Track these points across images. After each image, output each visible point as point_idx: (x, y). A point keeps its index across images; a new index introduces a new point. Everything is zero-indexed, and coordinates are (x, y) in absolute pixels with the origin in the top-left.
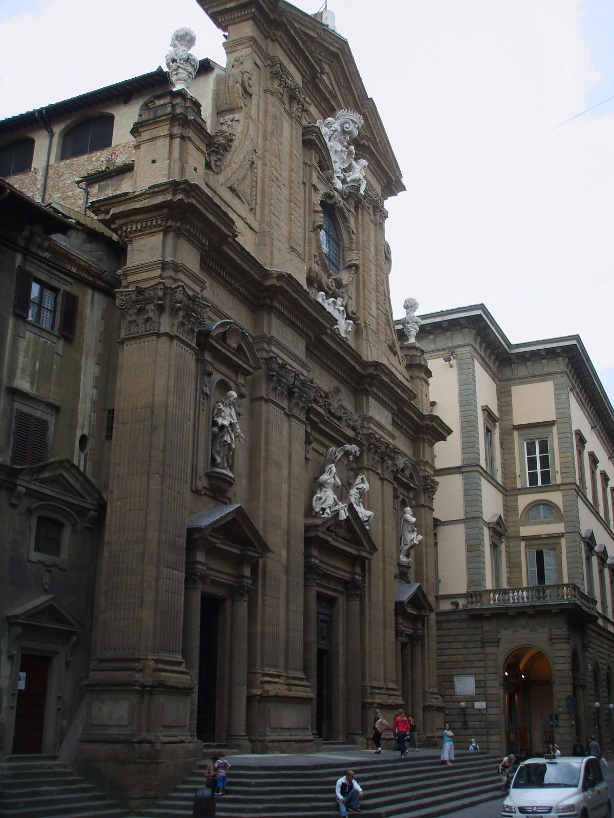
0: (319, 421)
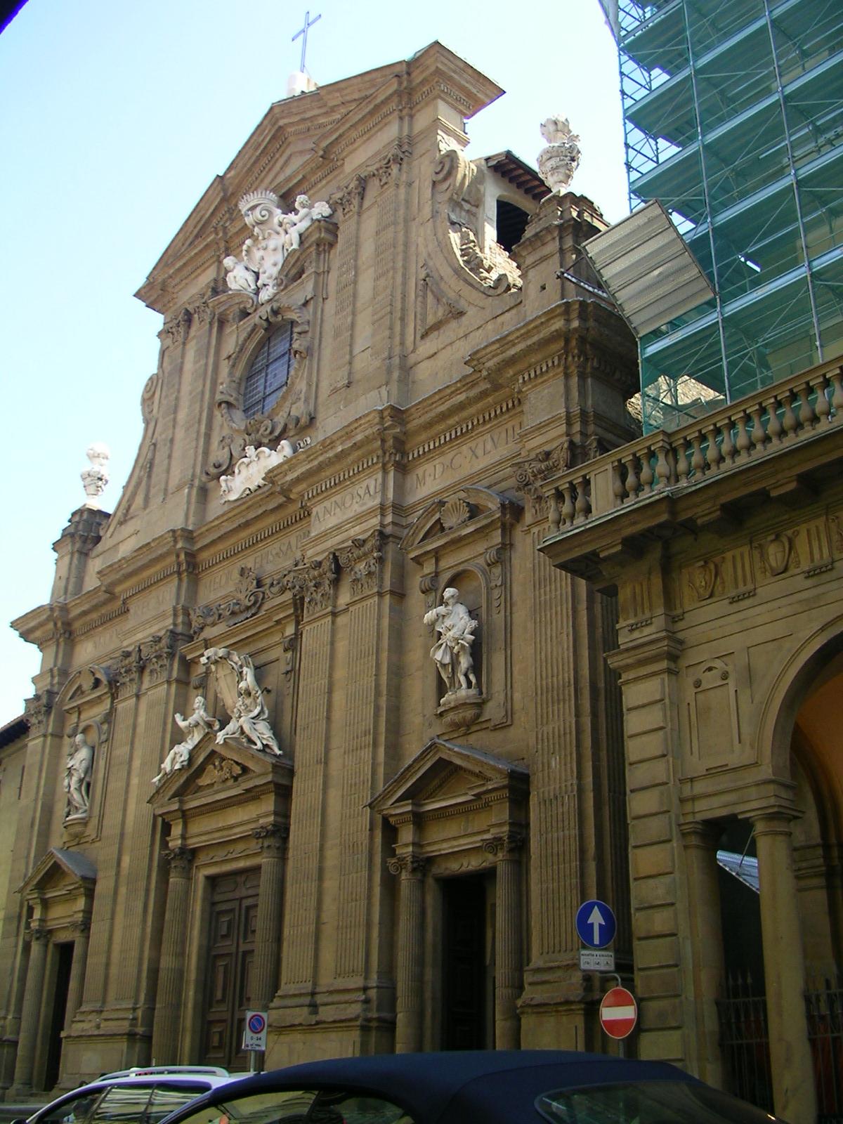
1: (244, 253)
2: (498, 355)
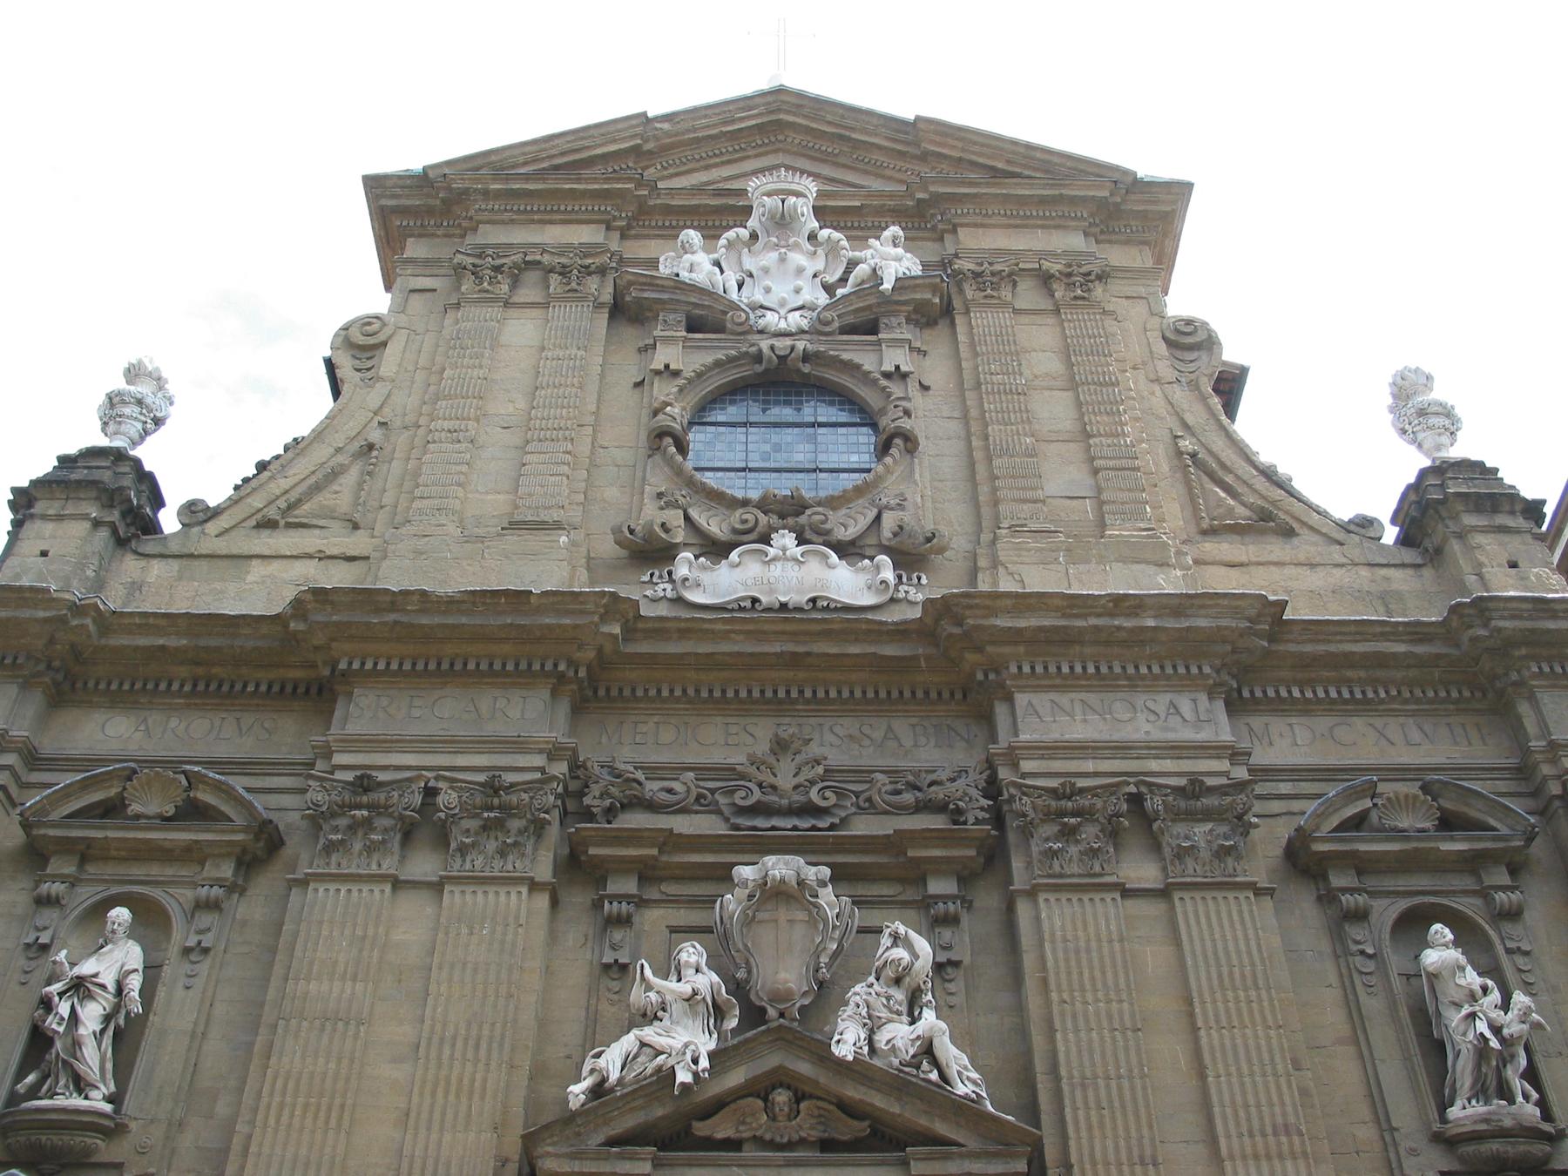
0: (655, 852)
1: (722, 241)
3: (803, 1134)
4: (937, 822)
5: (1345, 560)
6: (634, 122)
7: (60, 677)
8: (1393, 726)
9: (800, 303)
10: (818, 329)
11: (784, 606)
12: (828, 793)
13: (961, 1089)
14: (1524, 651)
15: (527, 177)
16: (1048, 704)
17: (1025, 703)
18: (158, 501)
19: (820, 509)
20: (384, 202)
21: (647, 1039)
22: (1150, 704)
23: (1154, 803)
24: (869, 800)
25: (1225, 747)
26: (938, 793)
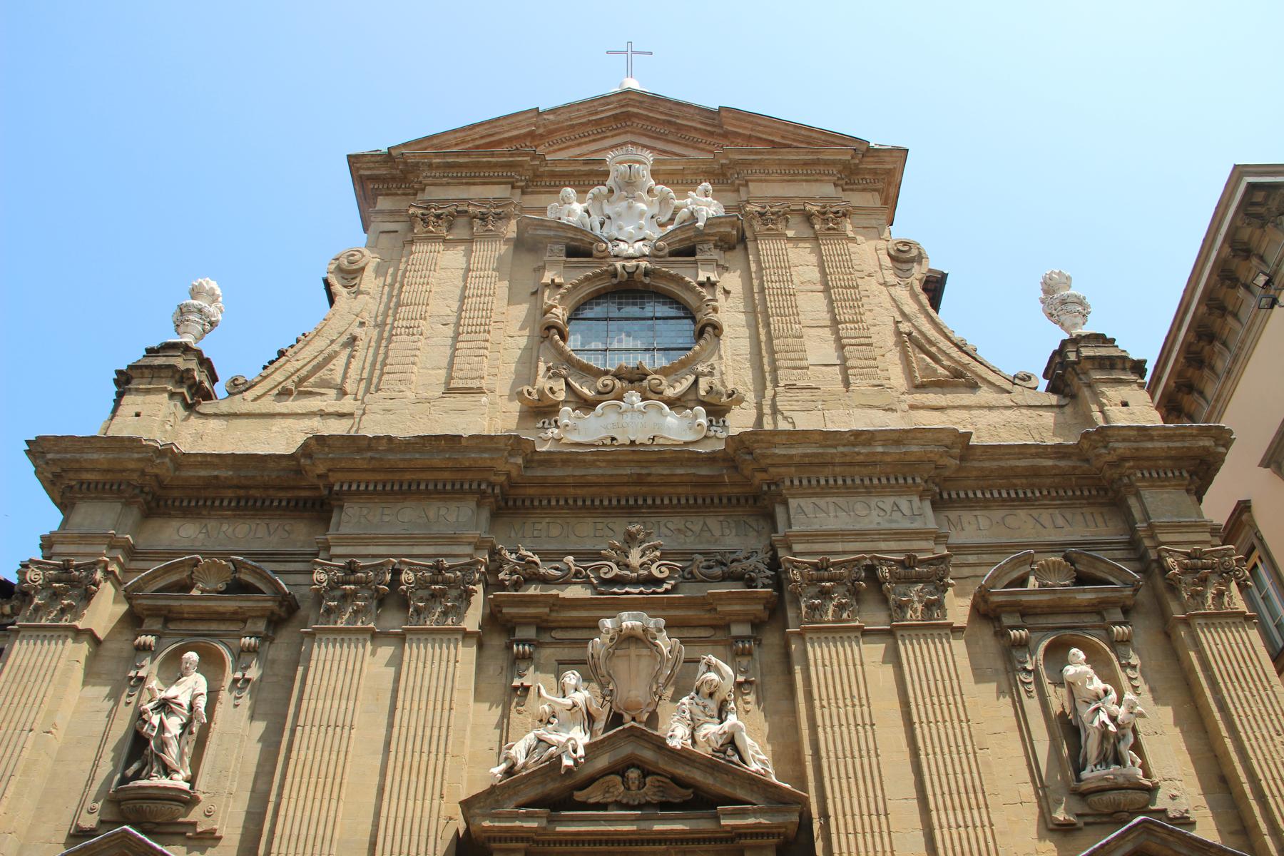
1: (589, 195)
2: (1130, 441)
3: (648, 799)
4: (736, 588)
5: (1012, 404)
6: (530, 115)
7: (149, 498)
8: (1045, 516)
9: (641, 237)
10: (655, 255)
11: (633, 443)
12: (663, 569)
13: (754, 767)
14: (1131, 463)
15: (458, 154)
16: (811, 505)
17: (796, 505)
18: (214, 379)
19: (657, 376)
20: (362, 172)
21: (544, 737)
22: (880, 504)
23: (884, 571)
24: (691, 573)
25: (931, 533)
26: (737, 567)
